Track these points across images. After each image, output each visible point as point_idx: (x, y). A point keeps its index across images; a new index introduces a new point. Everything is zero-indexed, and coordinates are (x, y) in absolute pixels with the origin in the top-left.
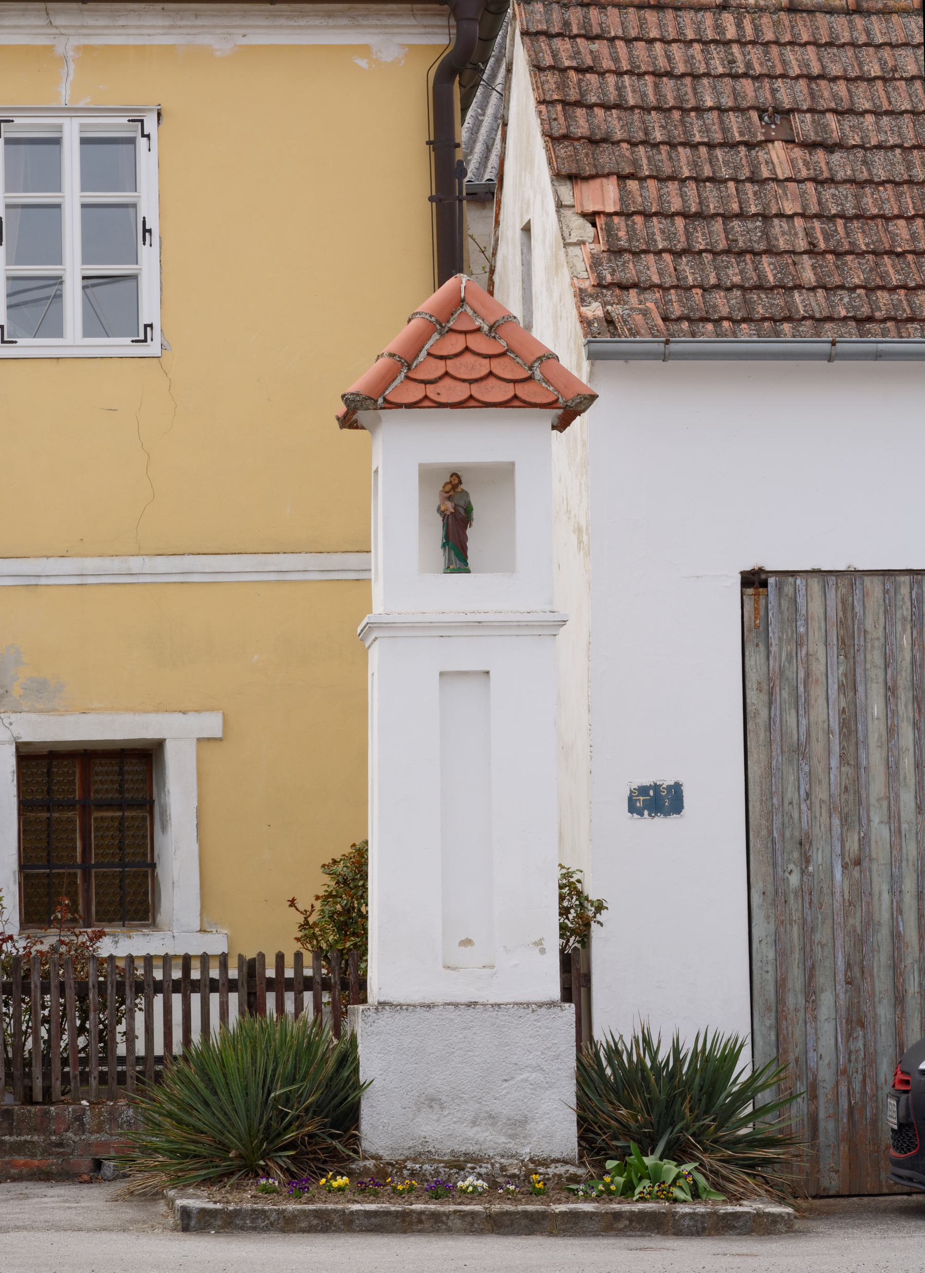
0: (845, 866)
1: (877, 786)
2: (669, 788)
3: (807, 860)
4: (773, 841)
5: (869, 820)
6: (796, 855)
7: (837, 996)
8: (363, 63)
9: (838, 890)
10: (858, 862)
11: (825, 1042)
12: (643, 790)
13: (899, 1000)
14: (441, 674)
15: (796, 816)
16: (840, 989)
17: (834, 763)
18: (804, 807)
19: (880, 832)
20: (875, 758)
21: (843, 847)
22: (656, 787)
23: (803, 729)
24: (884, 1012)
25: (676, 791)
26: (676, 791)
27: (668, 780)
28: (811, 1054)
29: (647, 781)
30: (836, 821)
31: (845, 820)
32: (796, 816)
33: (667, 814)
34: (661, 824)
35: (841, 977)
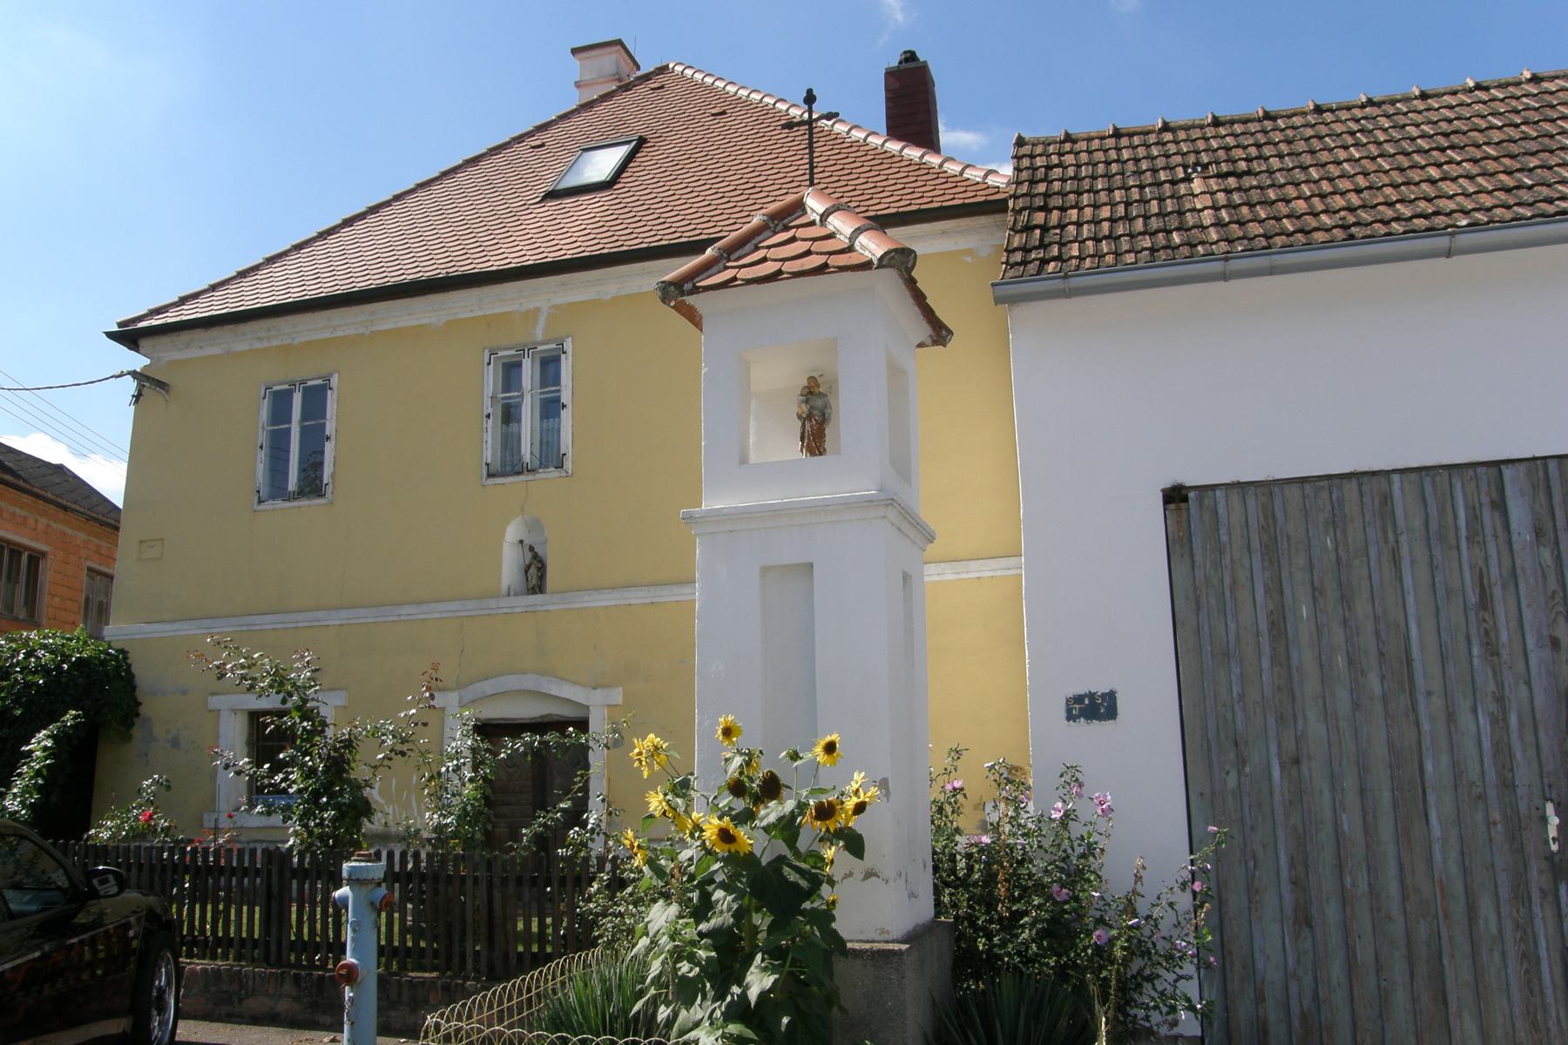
0: (1282, 766)
1: (1310, 687)
2: (1103, 696)
3: (1241, 761)
4: (1209, 741)
5: (1305, 719)
6: (1232, 756)
7: (1281, 897)
8: (969, 259)
9: (1277, 790)
10: (1297, 761)
11: (1270, 945)
12: (1078, 699)
13: (1345, 900)
14: (765, 570)
15: (1229, 716)
16: (1286, 888)
17: (1265, 663)
18: (1237, 708)
19: (1315, 728)
20: (1304, 656)
21: (1279, 746)
22: (1091, 696)
23: (1232, 635)
24: (1332, 912)
25: (1111, 697)
26: (1111, 697)
27: (1101, 688)
28: (1257, 955)
29: (1082, 691)
30: (1271, 721)
31: (1281, 719)
32: (1229, 716)
33: (1100, 717)
34: (1098, 728)
35: (1285, 874)
